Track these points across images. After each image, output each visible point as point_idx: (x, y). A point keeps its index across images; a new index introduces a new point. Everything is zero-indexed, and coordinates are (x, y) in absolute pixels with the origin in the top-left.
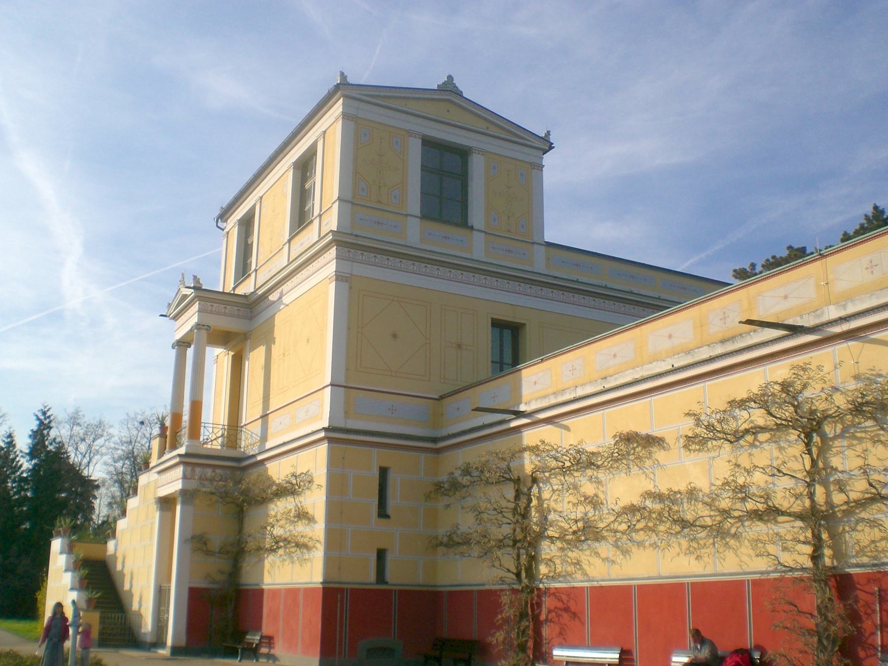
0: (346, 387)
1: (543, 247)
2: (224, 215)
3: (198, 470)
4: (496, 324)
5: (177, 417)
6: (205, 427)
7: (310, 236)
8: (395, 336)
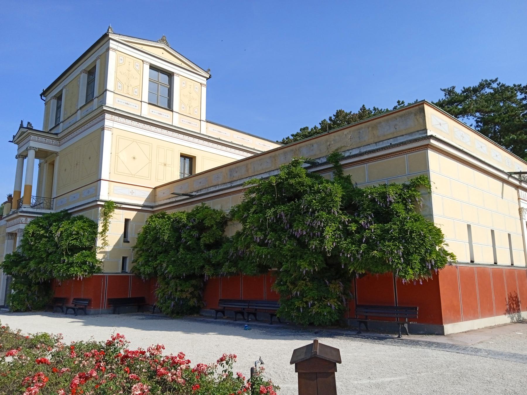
0: (109, 181)
1: (205, 123)
6: (33, 198)
8: (134, 158)
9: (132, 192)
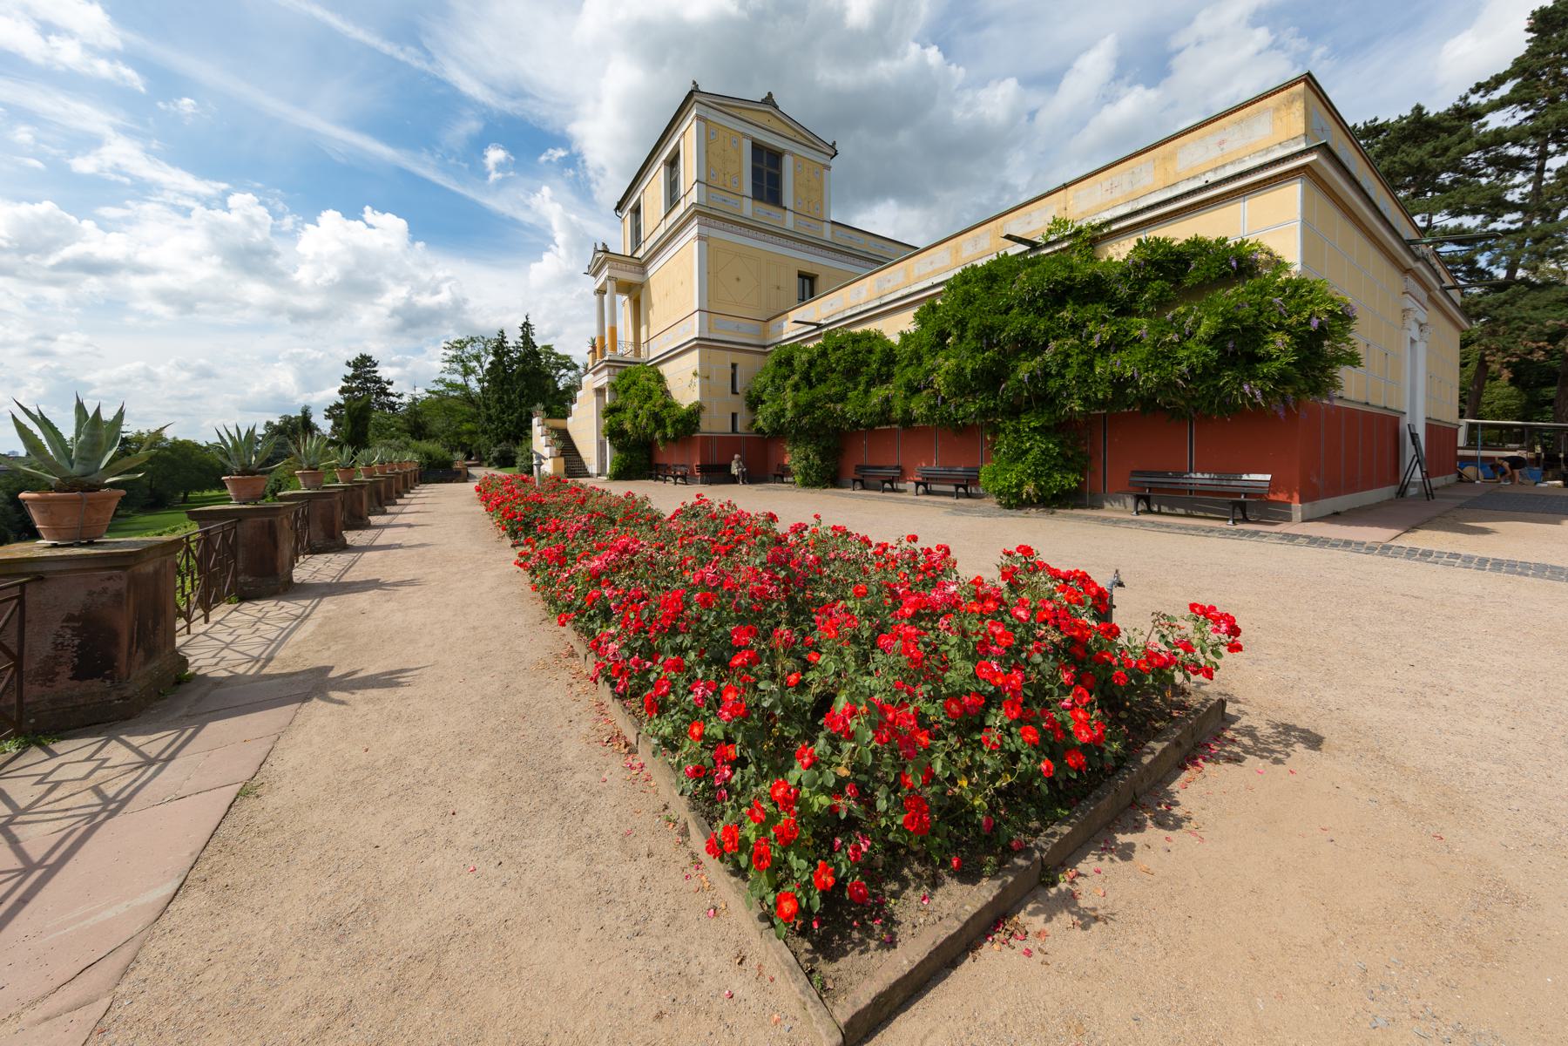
2: (620, 206)
3: (617, 370)
4: (802, 275)
5: (602, 339)
7: (680, 210)
8: (738, 279)
9: (738, 327)
